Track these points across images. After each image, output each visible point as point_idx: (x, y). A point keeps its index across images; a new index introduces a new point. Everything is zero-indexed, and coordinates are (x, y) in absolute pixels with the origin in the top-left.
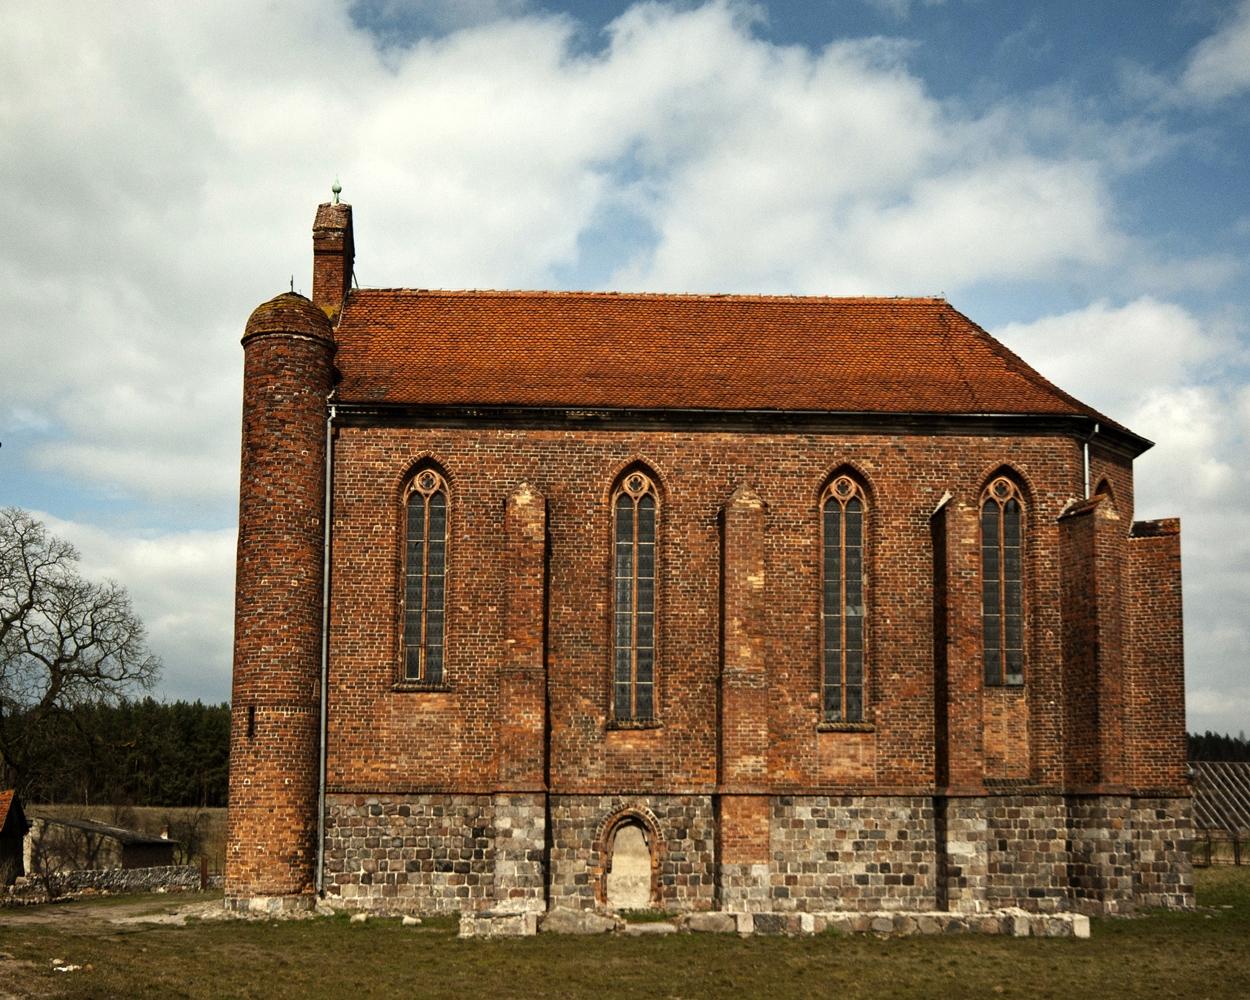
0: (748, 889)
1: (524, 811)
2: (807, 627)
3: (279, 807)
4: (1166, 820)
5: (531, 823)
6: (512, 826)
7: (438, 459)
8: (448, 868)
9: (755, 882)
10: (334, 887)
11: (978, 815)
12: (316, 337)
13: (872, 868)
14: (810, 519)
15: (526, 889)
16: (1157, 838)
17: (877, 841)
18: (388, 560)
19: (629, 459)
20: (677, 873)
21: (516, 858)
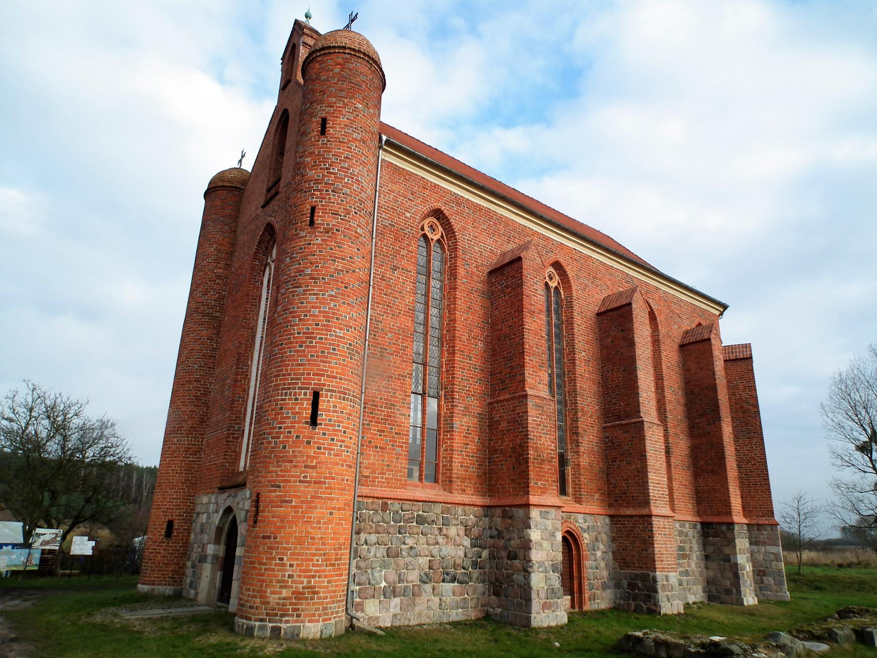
0: (670, 593)
5: (553, 535)
6: (542, 539)
8: (453, 580)
10: (358, 604)
18: (410, 282)
20: (594, 580)
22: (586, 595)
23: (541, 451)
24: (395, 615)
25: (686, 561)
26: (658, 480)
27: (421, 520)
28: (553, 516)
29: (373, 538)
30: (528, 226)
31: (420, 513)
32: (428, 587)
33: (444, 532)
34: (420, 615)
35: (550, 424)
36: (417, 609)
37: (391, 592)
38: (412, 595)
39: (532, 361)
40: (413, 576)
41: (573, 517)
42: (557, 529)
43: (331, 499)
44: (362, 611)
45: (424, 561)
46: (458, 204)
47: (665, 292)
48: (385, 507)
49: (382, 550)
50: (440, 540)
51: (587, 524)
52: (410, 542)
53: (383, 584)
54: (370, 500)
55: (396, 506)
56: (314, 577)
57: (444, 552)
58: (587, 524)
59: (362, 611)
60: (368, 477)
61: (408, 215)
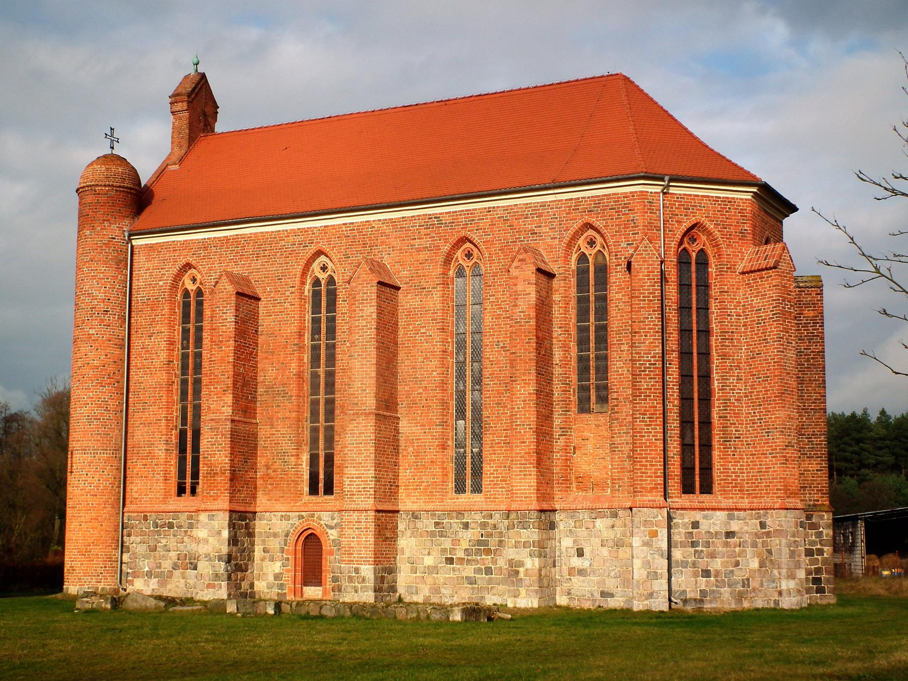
0: (359, 585)
1: (216, 524)
2: (434, 373)
3: (86, 522)
4: (767, 530)
5: (219, 533)
6: (208, 536)
7: (194, 263)
9: (364, 580)
11: (531, 527)
12: (113, 186)
13: (478, 571)
14: (437, 284)
15: (216, 583)
16: (760, 545)
17: (482, 548)
19: (313, 249)
21: (210, 560)
22: (328, 586)
23: (215, 466)
24: (153, 590)
25: (489, 557)
26: (358, 474)
27: (171, 526)
28: (220, 518)
29: (138, 539)
30: (281, 229)
31: (171, 520)
32: (177, 573)
33: (189, 533)
34: (170, 590)
35: (224, 441)
36: (169, 587)
37: (149, 574)
38: (165, 578)
39: (216, 388)
40: (167, 565)
41: (316, 516)
42: (223, 528)
43: (81, 516)
44: (133, 586)
45: (174, 555)
46: (206, 248)
47: (506, 208)
48: (146, 518)
49: (145, 546)
50: (186, 539)
51: (335, 521)
52: (164, 541)
53: (147, 569)
54: (136, 514)
55: (154, 516)
56: (73, 561)
57: (189, 548)
58: (335, 521)
59: (133, 586)
60: (137, 498)
61: (161, 283)
